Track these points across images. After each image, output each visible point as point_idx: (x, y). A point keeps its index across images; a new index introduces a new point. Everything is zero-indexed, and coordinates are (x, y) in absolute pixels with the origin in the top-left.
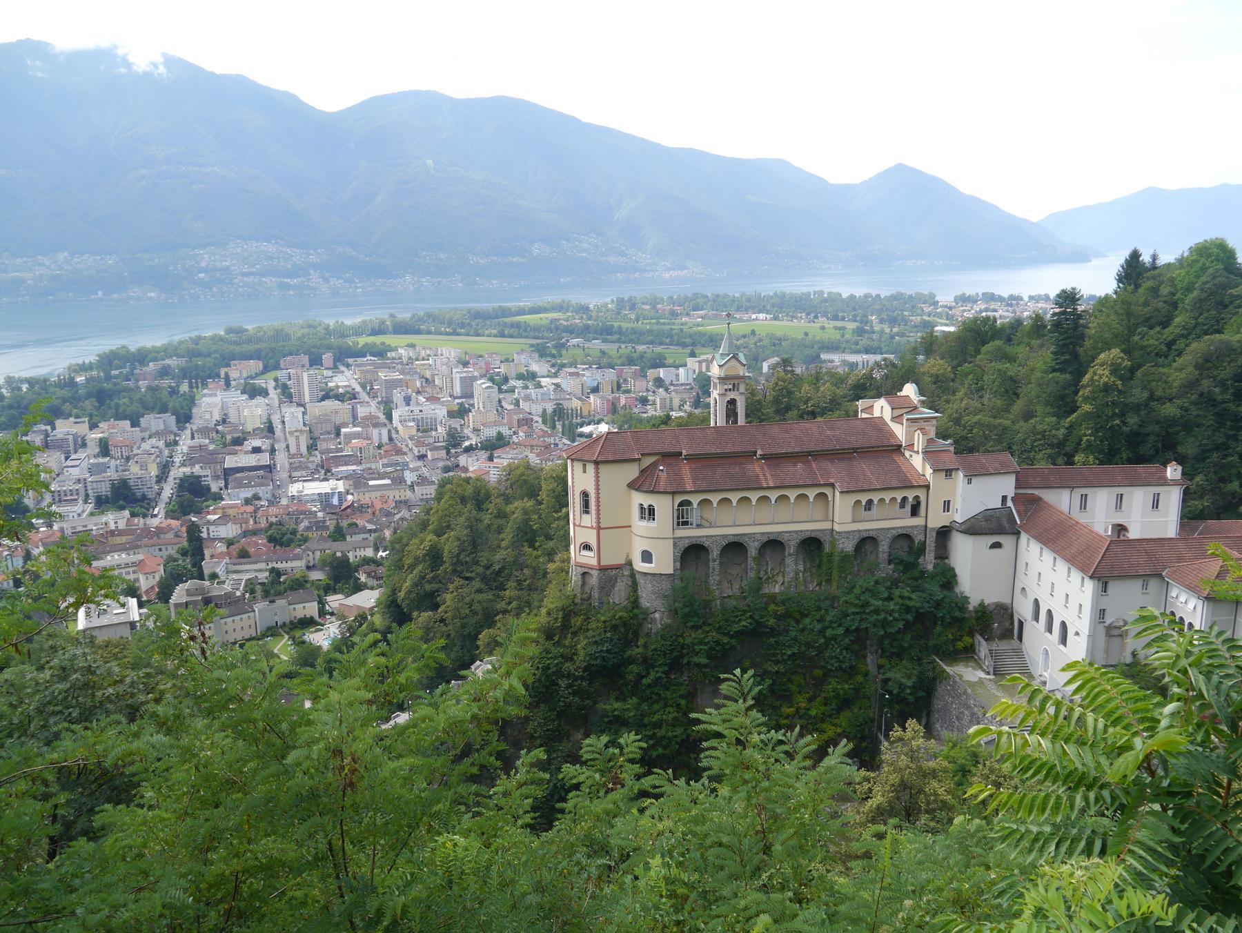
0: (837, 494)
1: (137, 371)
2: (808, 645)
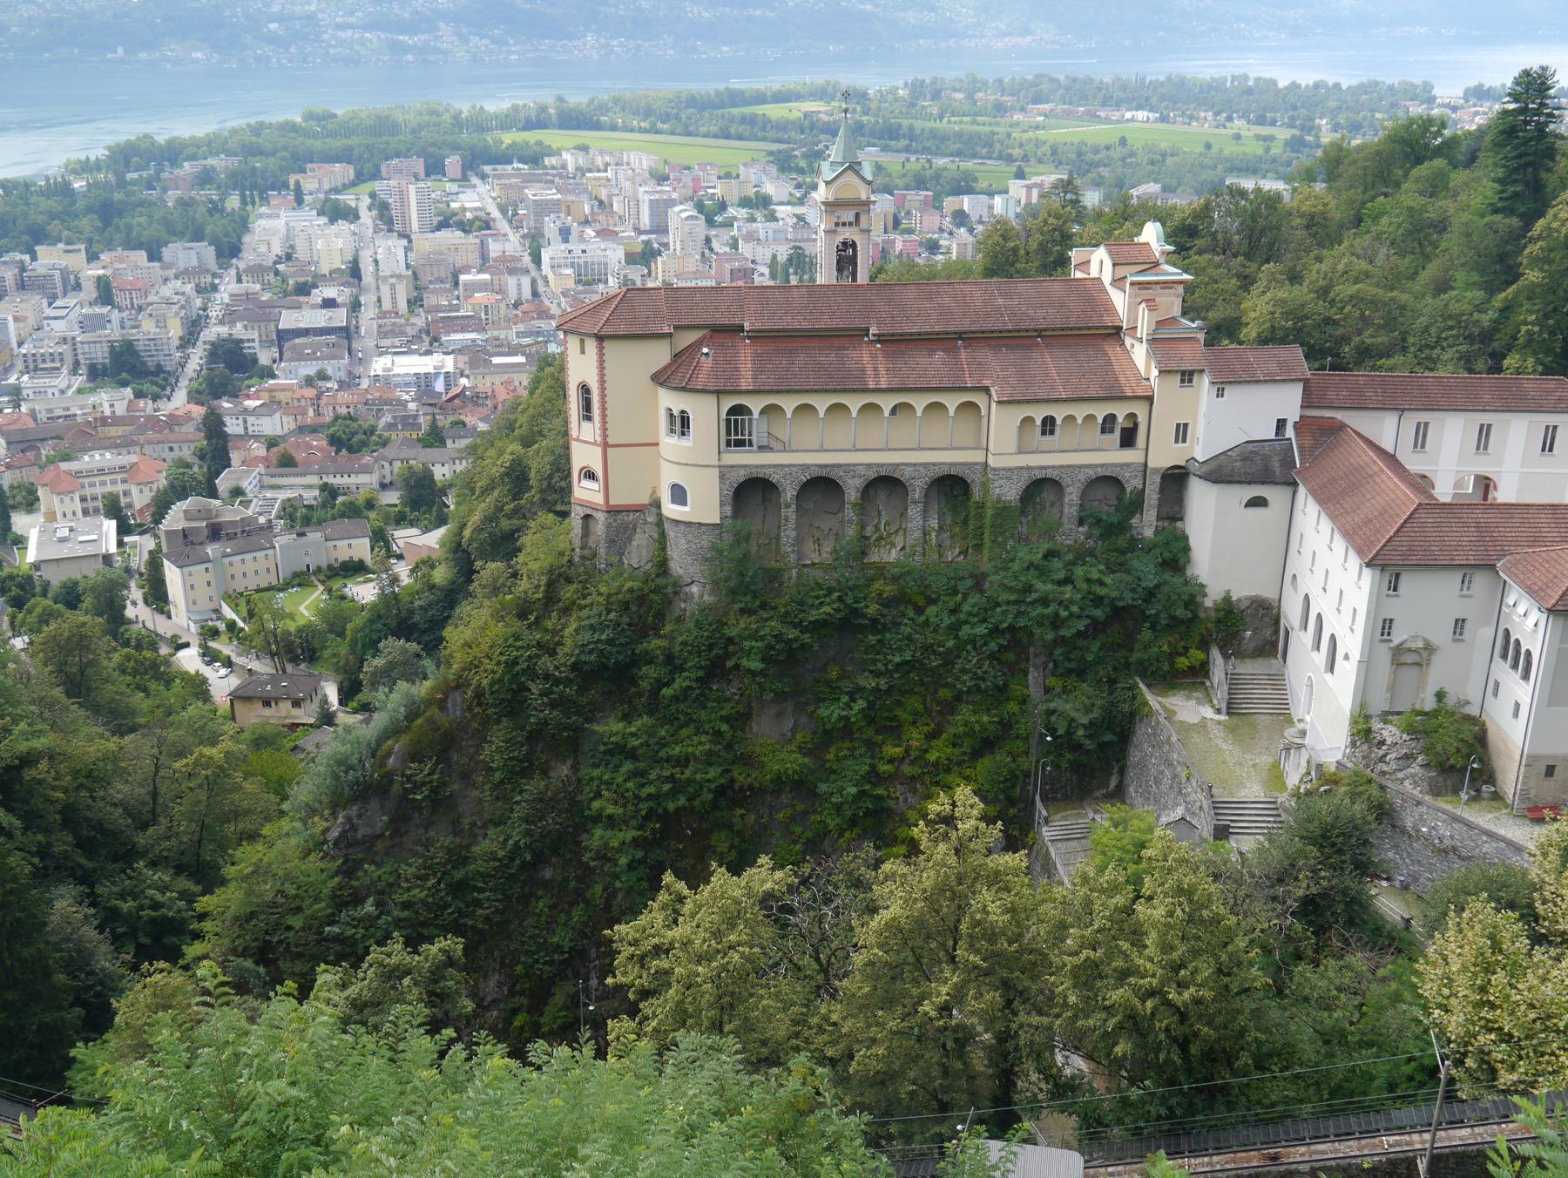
0: (994, 405)
1: (165, 175)
2: (928, 649)
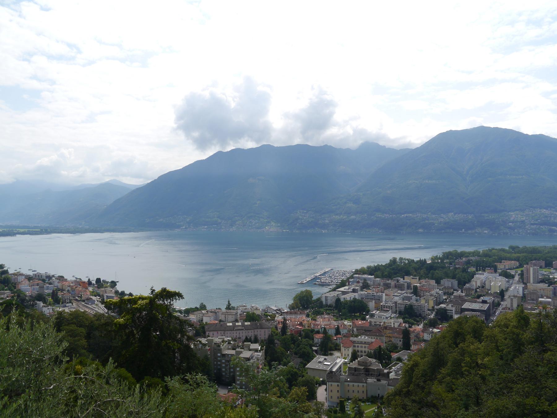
1: (457, 261)
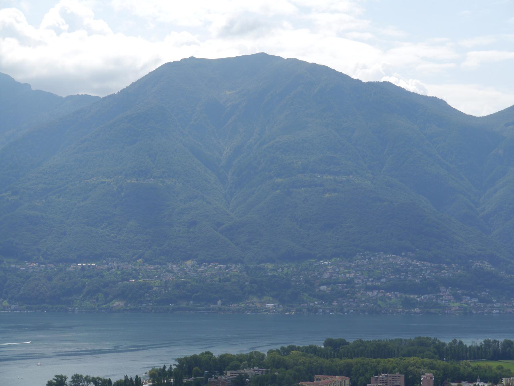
1: (212, 379)
